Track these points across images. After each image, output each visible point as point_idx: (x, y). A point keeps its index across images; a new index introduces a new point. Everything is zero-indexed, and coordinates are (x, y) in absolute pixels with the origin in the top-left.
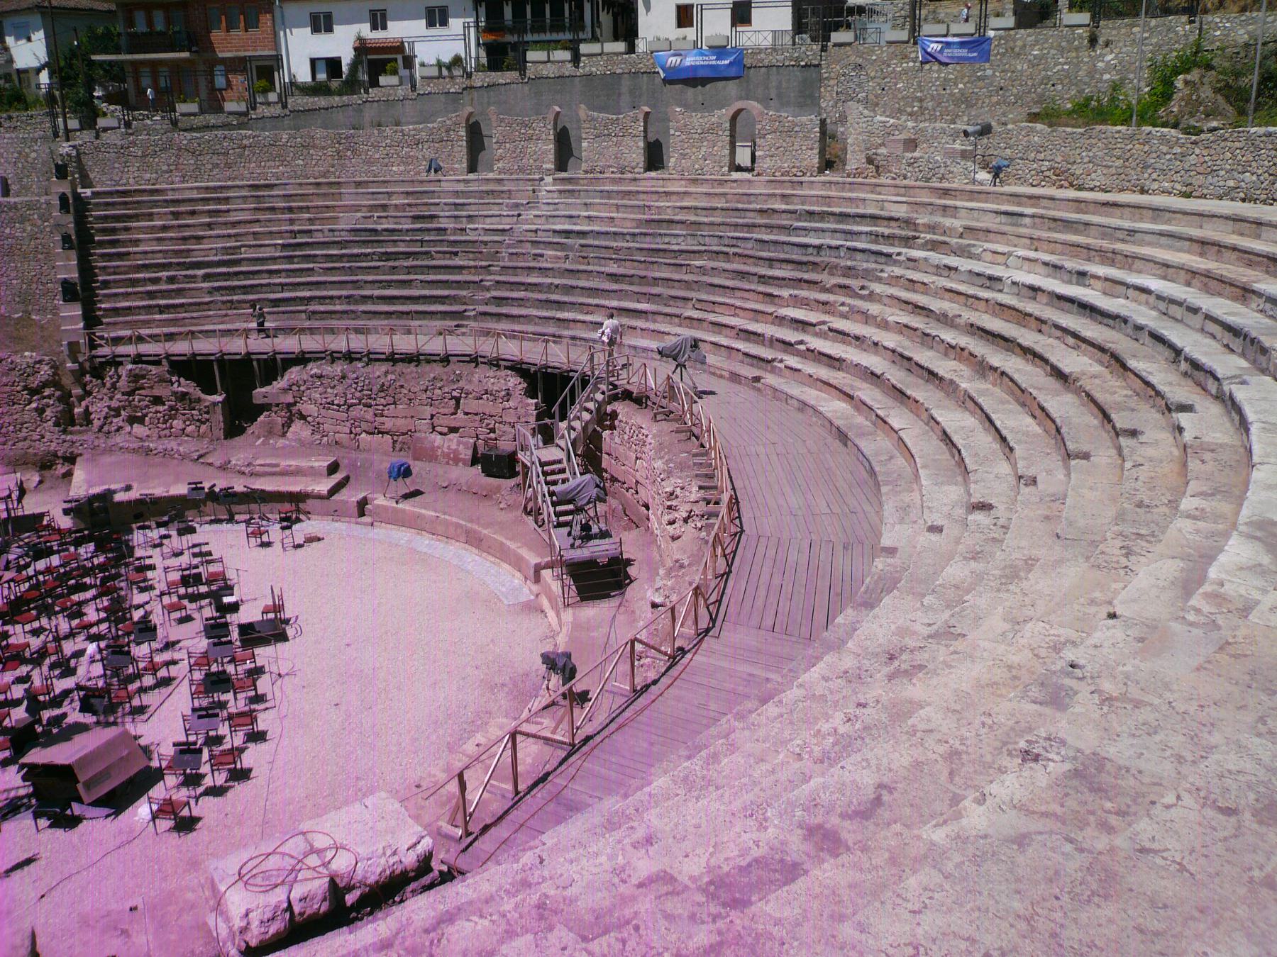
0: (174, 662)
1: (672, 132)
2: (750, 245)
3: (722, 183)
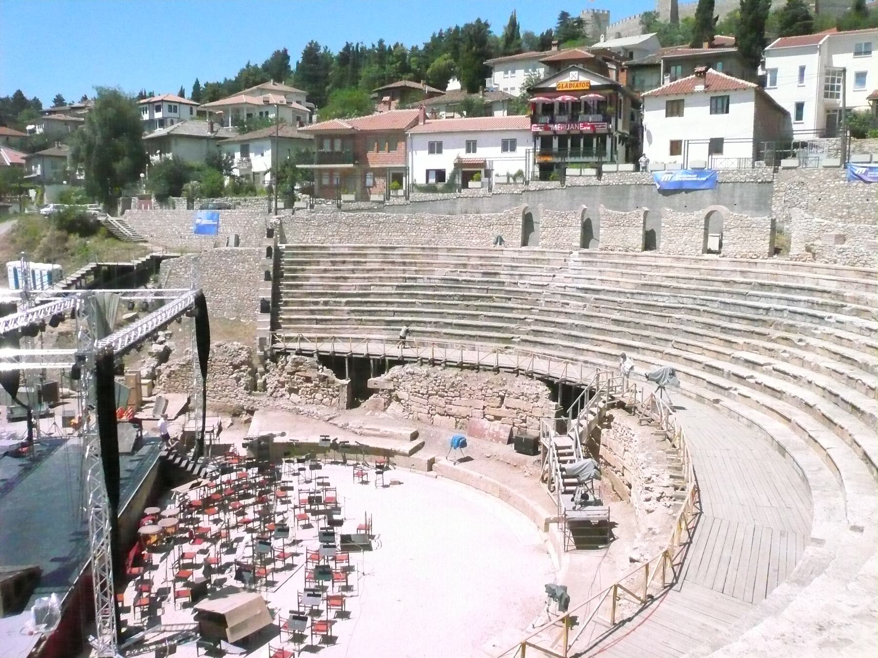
0: (297, 555)
1: (663, 225)
2: (716, 305)
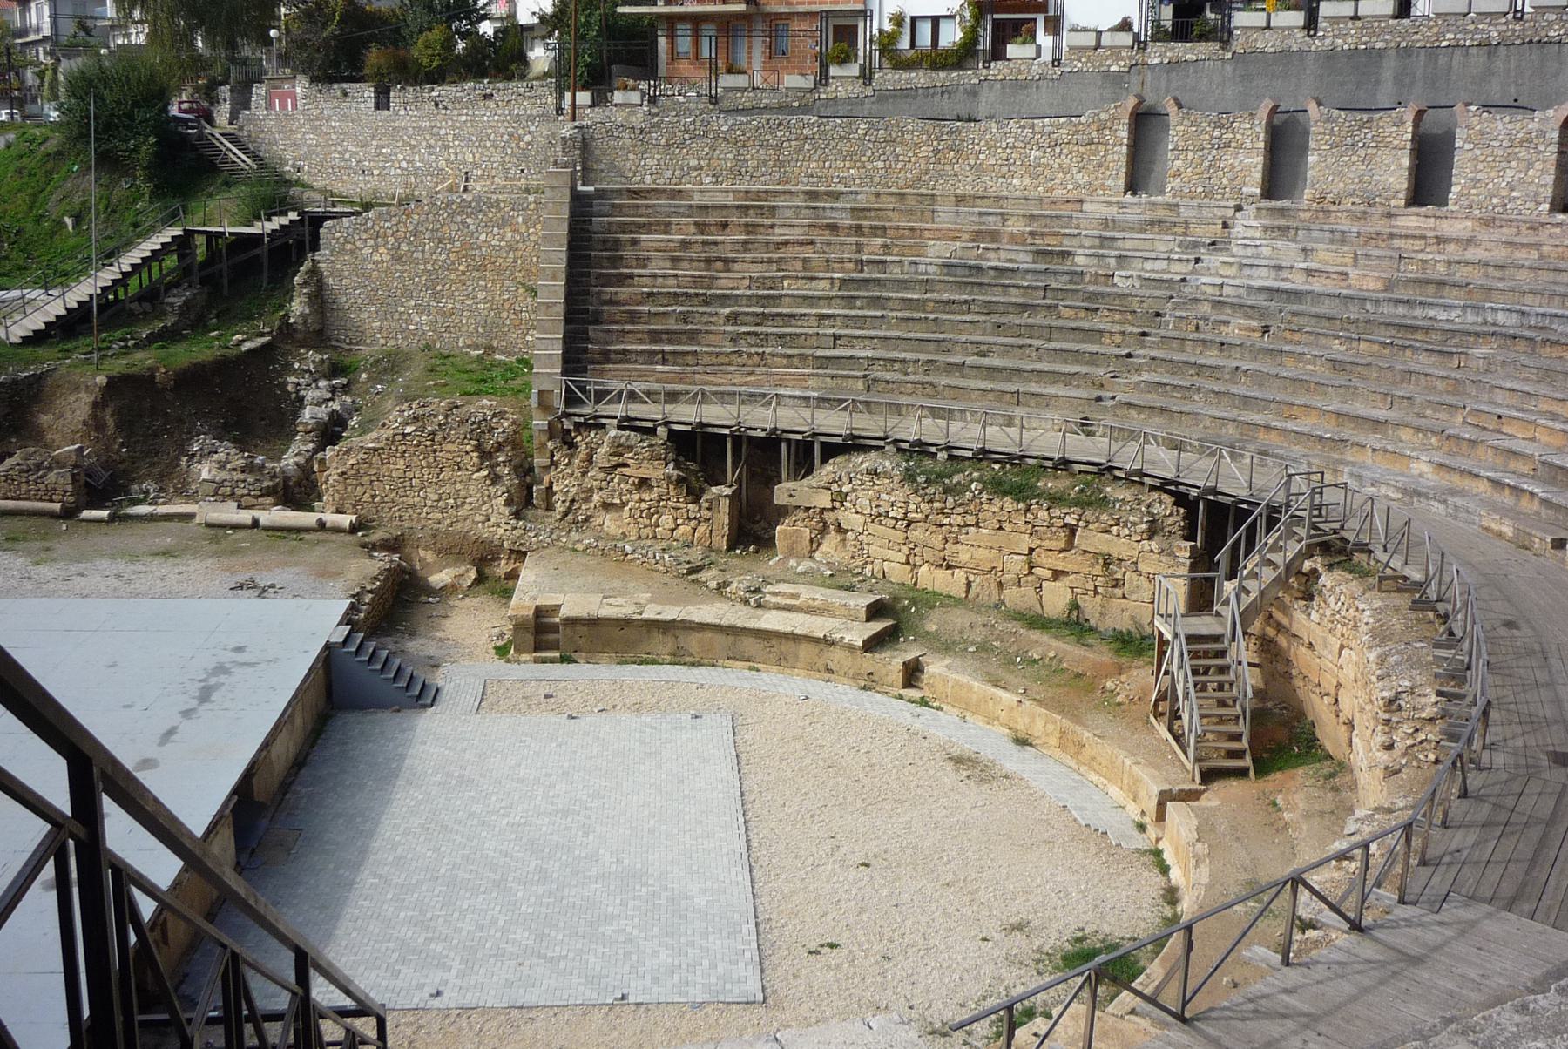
1: (1458, 143)
3: (1535, 227)
